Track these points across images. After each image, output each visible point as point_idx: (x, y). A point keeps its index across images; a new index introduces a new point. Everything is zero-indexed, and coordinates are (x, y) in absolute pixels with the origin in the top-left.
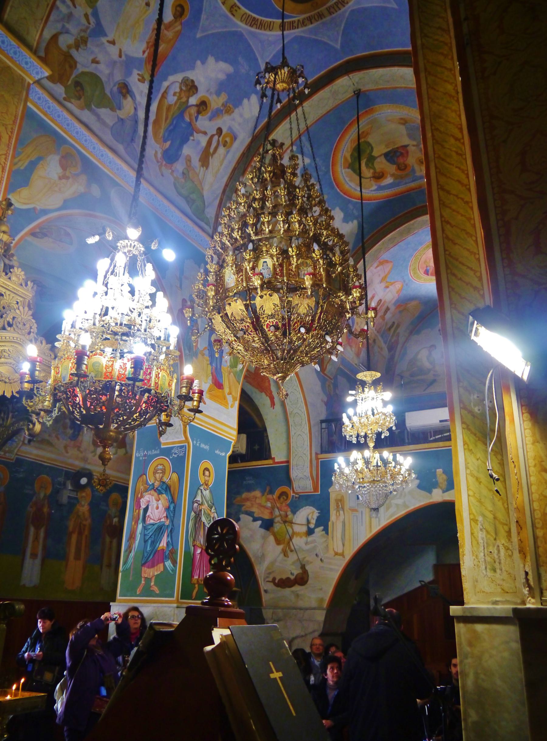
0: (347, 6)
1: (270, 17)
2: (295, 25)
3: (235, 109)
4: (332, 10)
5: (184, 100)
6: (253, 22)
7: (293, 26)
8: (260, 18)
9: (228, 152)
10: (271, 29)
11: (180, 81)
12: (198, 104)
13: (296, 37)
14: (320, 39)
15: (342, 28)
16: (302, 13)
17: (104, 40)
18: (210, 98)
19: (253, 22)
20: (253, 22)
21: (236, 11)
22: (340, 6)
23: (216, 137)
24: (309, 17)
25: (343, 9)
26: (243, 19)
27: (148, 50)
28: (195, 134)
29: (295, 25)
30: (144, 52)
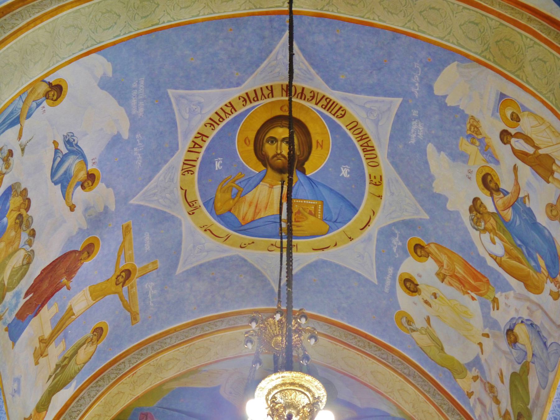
0: (243, 93)
1: (346, 134)
2: (324, 102)
3: (467, 115)
4: (266, 92)
5: (492, 221)
6: (369, 149)
7: (328, 103)
8: (358, 145)
9: (525, 109)
10: (355, 124)
11: (478, 232)
12: (489, 193)
13: (333, 88)
14: (306, 63)
15: (266, 62)
16: (307, 110)
17: (483, 358)
18: (475, 170)
19: (368, 149)
20: (369, 149)
21: (375, 177)
22: (252, 96)
23: (513, 140)
24: (301, 98)
25: (250, 90)
26: (376, 164)
27: (469, 291)
28: (521, 195)
29: (324, 102)
30: (473, 299)
